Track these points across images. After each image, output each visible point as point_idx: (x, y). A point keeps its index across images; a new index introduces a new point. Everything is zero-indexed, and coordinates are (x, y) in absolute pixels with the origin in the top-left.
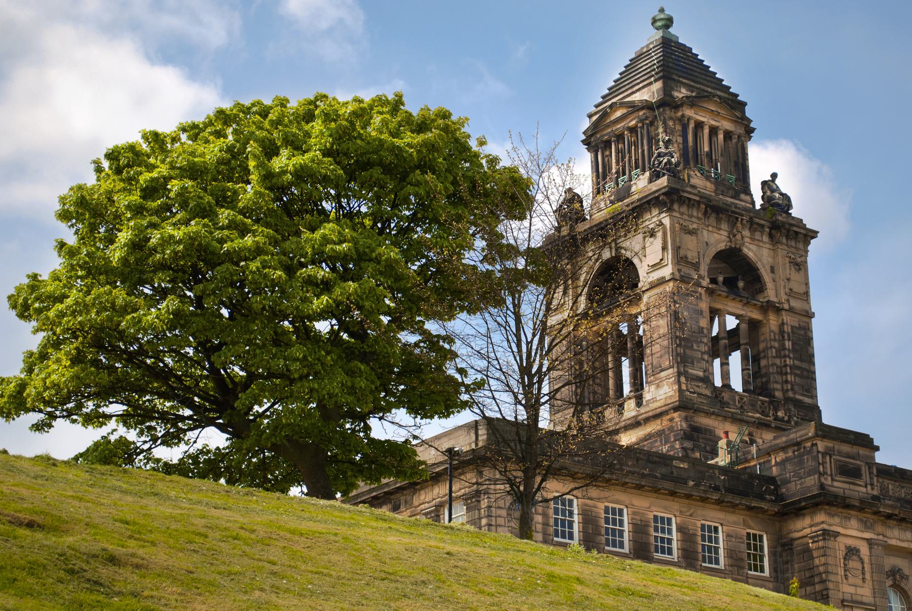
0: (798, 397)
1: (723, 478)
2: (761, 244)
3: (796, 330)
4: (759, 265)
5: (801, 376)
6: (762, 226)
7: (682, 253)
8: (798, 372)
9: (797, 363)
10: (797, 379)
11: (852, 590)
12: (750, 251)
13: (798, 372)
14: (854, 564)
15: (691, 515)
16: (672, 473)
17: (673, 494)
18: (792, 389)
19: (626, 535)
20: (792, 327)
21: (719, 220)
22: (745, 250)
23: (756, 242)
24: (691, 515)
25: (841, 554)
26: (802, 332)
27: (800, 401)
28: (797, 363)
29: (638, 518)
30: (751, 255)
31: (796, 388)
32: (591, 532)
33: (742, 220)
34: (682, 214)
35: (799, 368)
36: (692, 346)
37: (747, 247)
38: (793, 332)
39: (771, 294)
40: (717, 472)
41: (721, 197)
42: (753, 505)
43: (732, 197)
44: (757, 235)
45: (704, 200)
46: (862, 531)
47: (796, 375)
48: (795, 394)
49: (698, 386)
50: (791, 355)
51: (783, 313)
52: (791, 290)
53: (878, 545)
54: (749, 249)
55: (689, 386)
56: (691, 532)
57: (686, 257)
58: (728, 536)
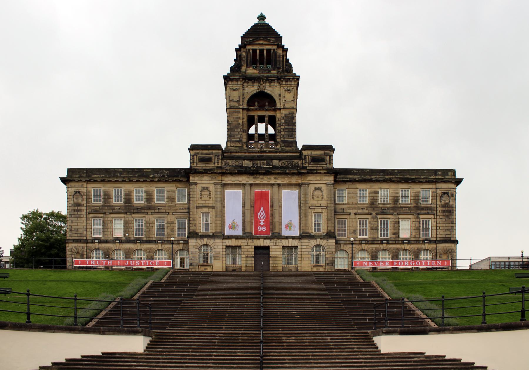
0: (286, 139)
1: (167, 172)
2: (274, 87)
3: (286, 115)
4: (273, 95)
5: (288, 132)
6: (274, 80)
7: (231, 99)
8: (287, 130)
9: (286, 127)
10: (286, 133)
11: (204, 202)
12: (268, 90)
13: (287, 130)
14: (206, 193)
15: (151, 187)
16: (144, 174)
17: (145, 181)
18: (283, 137)
19: (123, 197)
20: (285, 114)
21: (253, 83)
22: (266, 91)
23: (272, 87)
24: (151, 187)
25: (199, 191)
26: (291, 115)
27: (287, 141)
28: (286, 127)
29: (127, 191)
30: (269, 92)
31: (285, 136)
32: (106, 198)
33: (263, 80)
34: (233, 85)
35: (287, 129)
36: (234, 130)
37: (267, 90)
38: (285, 116)
39: (278, 105)
40: (164, 171)
41: (262, 74)
42: (175, 179)
43: (267, 73)
44: (273, 84)
45: (241, 77)
46: (210, 181)
47: (286, 131)
48: (284, 138)
49: (236, 144)
50: (284, 125)
51: (281, 110)
52: (285, 100)
53: (219, 184)
54: (268, 90)
55: (231, 145)
56: (150, 192)
57: (233, 100)
58: (168, 191)
